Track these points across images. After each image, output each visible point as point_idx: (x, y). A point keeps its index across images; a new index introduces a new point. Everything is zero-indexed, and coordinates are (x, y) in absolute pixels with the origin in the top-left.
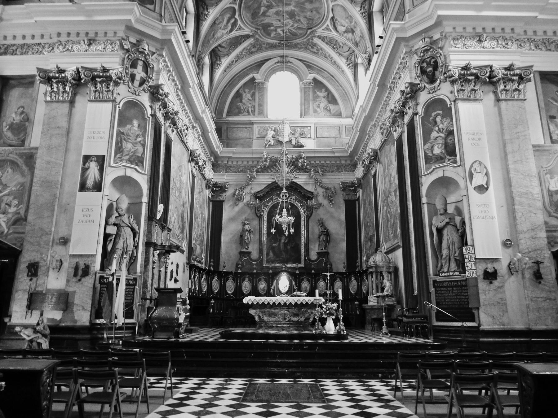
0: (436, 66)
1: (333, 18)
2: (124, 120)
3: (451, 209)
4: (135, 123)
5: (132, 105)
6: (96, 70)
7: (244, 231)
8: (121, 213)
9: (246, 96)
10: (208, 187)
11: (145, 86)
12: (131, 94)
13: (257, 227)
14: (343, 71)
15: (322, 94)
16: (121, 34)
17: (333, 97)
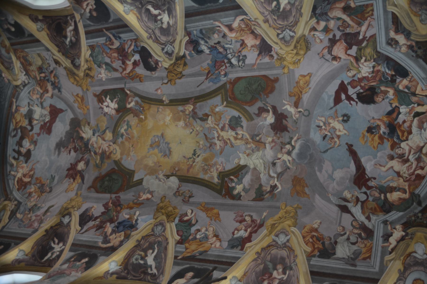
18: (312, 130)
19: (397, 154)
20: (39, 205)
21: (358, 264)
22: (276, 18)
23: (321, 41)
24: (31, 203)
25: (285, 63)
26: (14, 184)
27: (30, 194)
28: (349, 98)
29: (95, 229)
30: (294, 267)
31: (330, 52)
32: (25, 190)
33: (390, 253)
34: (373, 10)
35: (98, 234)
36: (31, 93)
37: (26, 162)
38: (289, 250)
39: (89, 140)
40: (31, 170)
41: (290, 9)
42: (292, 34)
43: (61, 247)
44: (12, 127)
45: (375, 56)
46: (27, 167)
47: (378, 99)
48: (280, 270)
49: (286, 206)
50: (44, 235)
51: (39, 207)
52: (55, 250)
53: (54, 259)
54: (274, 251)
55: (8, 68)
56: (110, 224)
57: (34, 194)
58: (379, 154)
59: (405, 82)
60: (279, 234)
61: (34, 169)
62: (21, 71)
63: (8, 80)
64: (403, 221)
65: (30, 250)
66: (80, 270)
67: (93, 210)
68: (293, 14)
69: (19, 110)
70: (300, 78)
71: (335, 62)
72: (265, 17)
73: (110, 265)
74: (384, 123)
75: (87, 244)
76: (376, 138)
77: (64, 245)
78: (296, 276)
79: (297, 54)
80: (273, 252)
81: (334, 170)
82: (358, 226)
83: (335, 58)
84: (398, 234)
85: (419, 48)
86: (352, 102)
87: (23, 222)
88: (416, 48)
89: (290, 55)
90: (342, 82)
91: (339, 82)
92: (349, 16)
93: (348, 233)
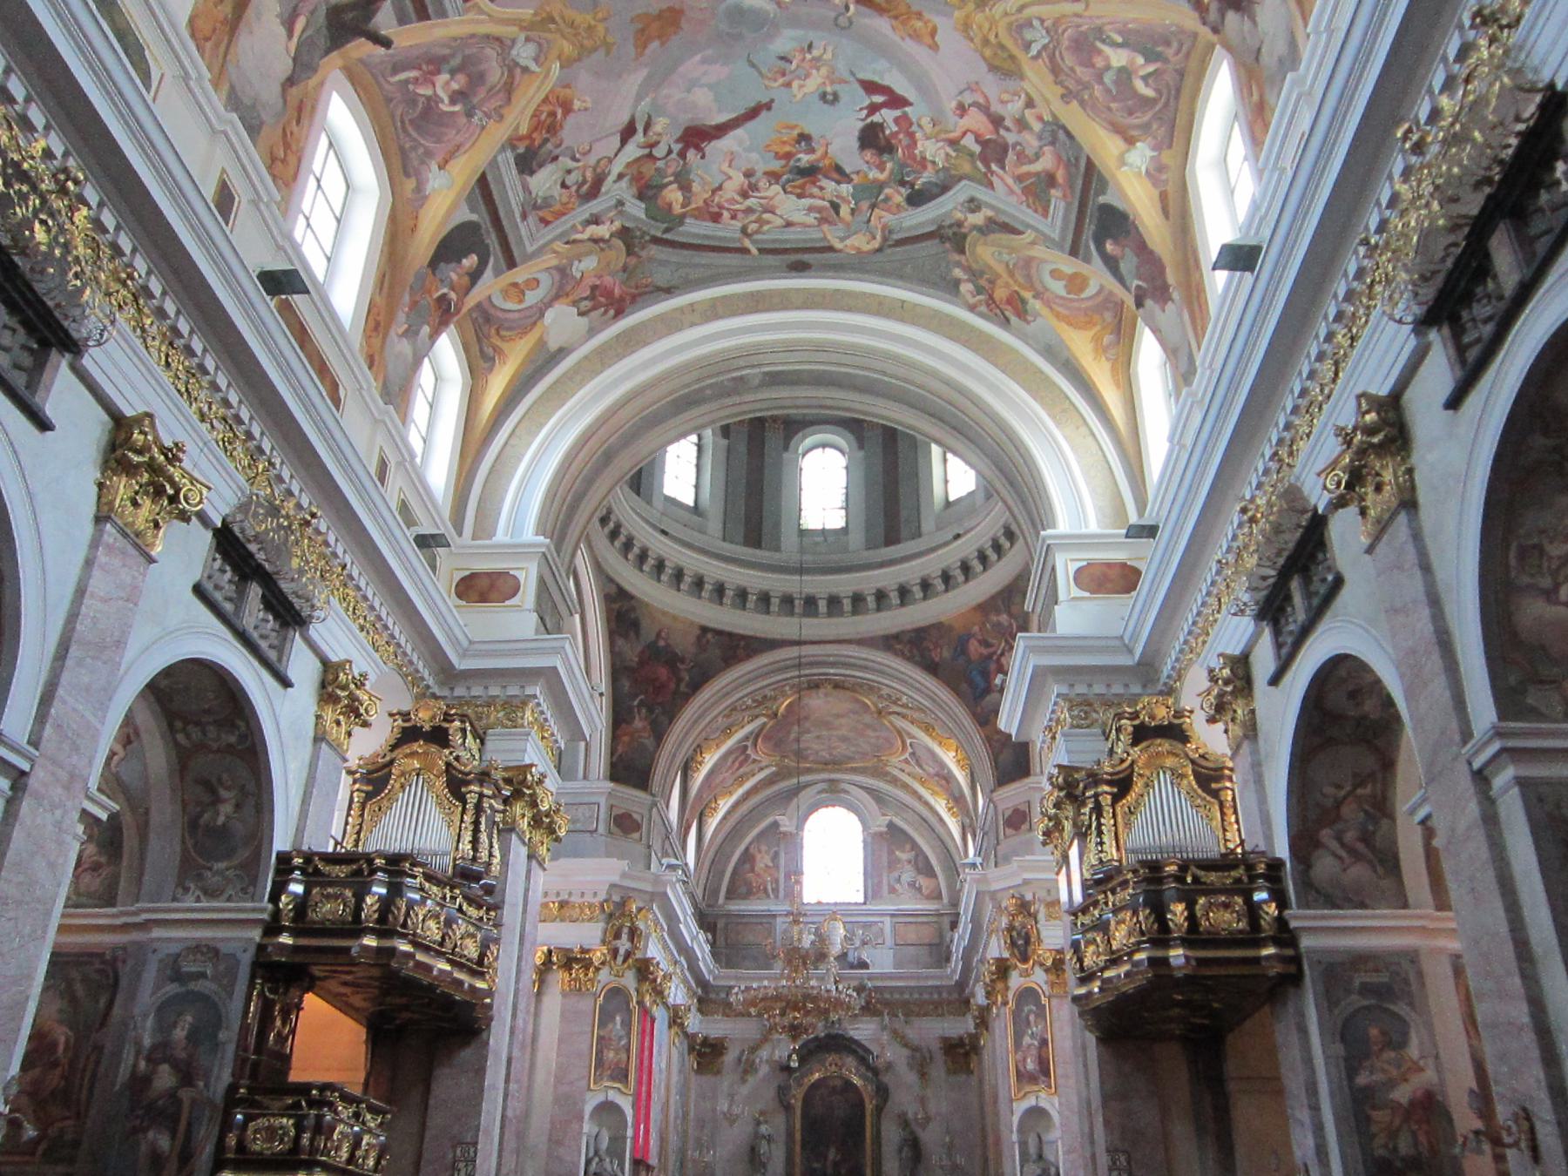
0: (1027, 941)
1: (913, 754)
2: (606, 1018)
3: (1049, 1155)
4: (618, 1019)
5: (616, 993)
6: (571, 950)
7: (757, 1136)
8: (604, 1156)
9: (763, 860)
10: (691, 1049)
11: (630, 961)
12: (612, 978)
13: (782, 1128)
14: (941, 820)
15: (903, 856)
16: (602, 896)
17: (926, 858)
18: (800, 33)
19: (757, 181)
21: (530, 219)
22: (1084, 28)
23: (1003, 102)
25: (971, 6)
28: (873, 109)
30: (475, 119)
31: (975, 104)
33: (567, 243)
34: (1036, 211)
38: (505, 83)
41: (1093, 66)
42: (1034, 51)
45: (953, 172)
47: (868, 155)
48: (455, 86)
49: (604, 19)
54: (491, 53)
58: (754, 156)
59: (899, 199)
60: (534, 41)
64: (627, 225)
68: (1078, 69)
70: (930, 25)
71: (954, 104)
72: (1090, 18)
74: (818, 160)
76: (787, 148)
78: (459, 139)
79: (986, 42)
80: (489, 51)
81: (711, 87)
82: (599, 170)
83: (962, 110)
84: (603, 231)
85: (954, 234)
86: (865, 112)
88: (955, 229)
89: (987, 26)
90: (911, 104)
91: (911, 99)
92: (1037, 174)
93: (580, 164)
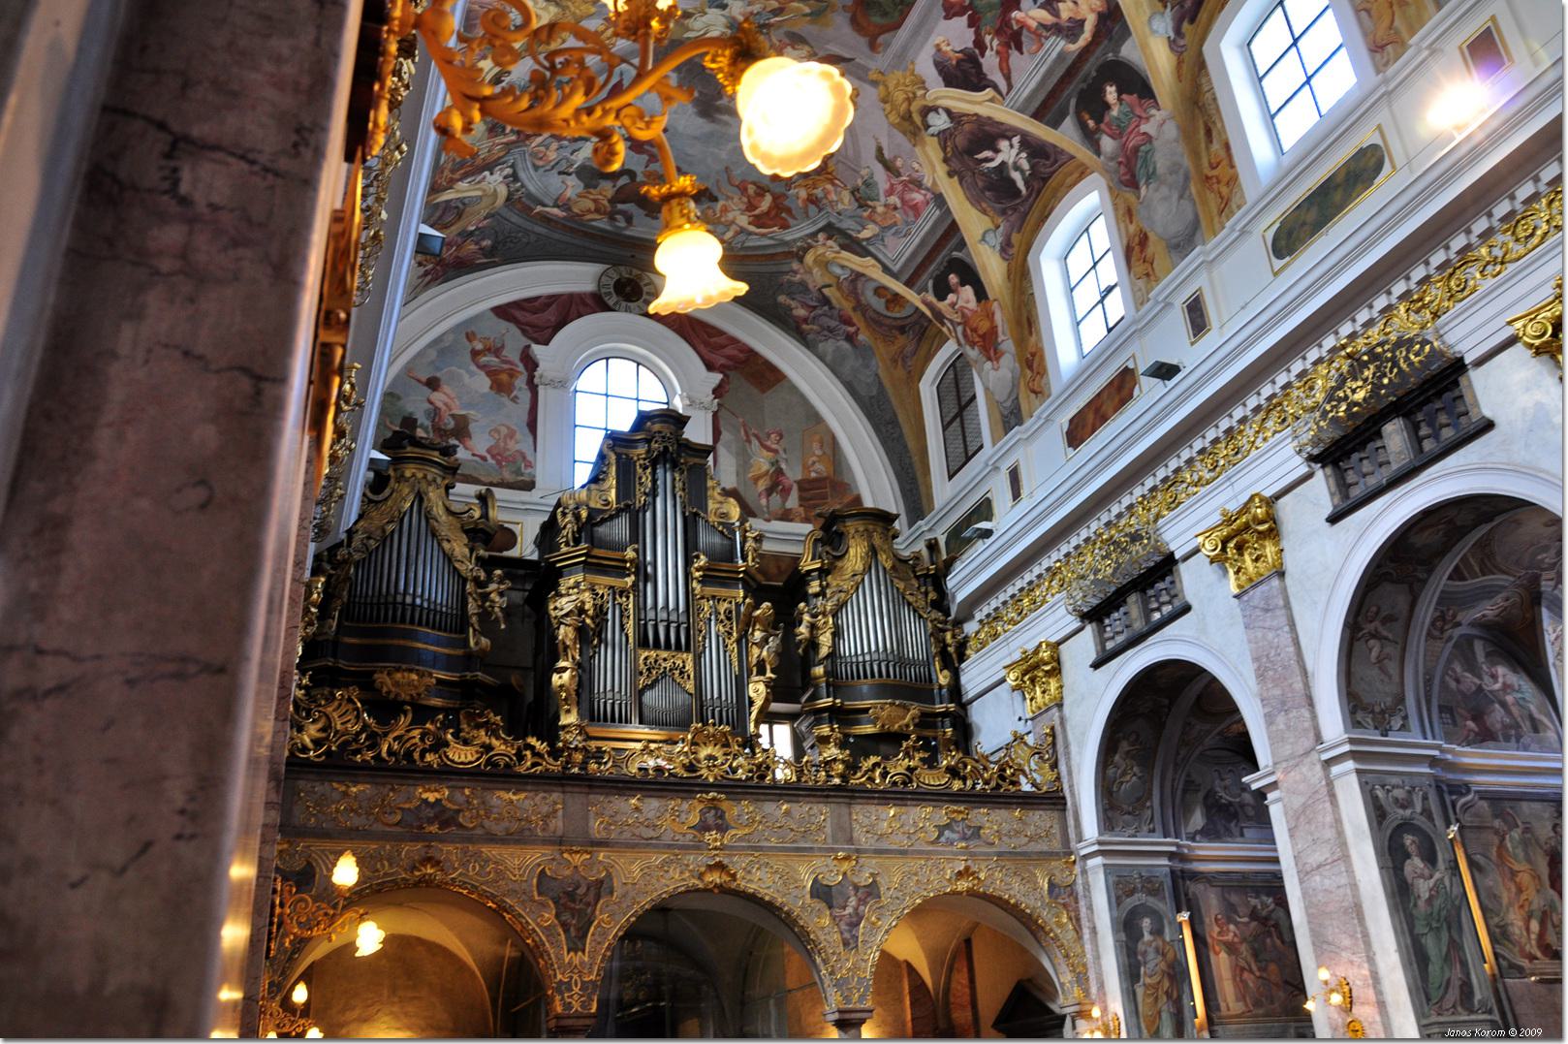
20: (860, 182)
24: (843, 203)
26: (763, 235)
27: (812, 200)
29: (1014, 54)
32: (794, 212)
35: (1034, 47)
36: (540, 163)
37: (715, 199)
39: (733, 24)
40: (743, 190)
43: (1011, 146)
44: (603, 224)
46: (728, 198)
50: (961, 183)
51: (864, 183)
52: (1011, 162)
53: (1032, 167)
55: (460, 215)
56: (1019, 9)
57: (818, 192)
61: (743, 181)
62: (479, 182)
63: (485, 218)
65: (986, 218)
66: (1145, 111)
67: (945, 48)
69: (569, 199)
73: (1157, 32)
75: (1054, 80)
77: (1009, 139)
87: (895, 224)
